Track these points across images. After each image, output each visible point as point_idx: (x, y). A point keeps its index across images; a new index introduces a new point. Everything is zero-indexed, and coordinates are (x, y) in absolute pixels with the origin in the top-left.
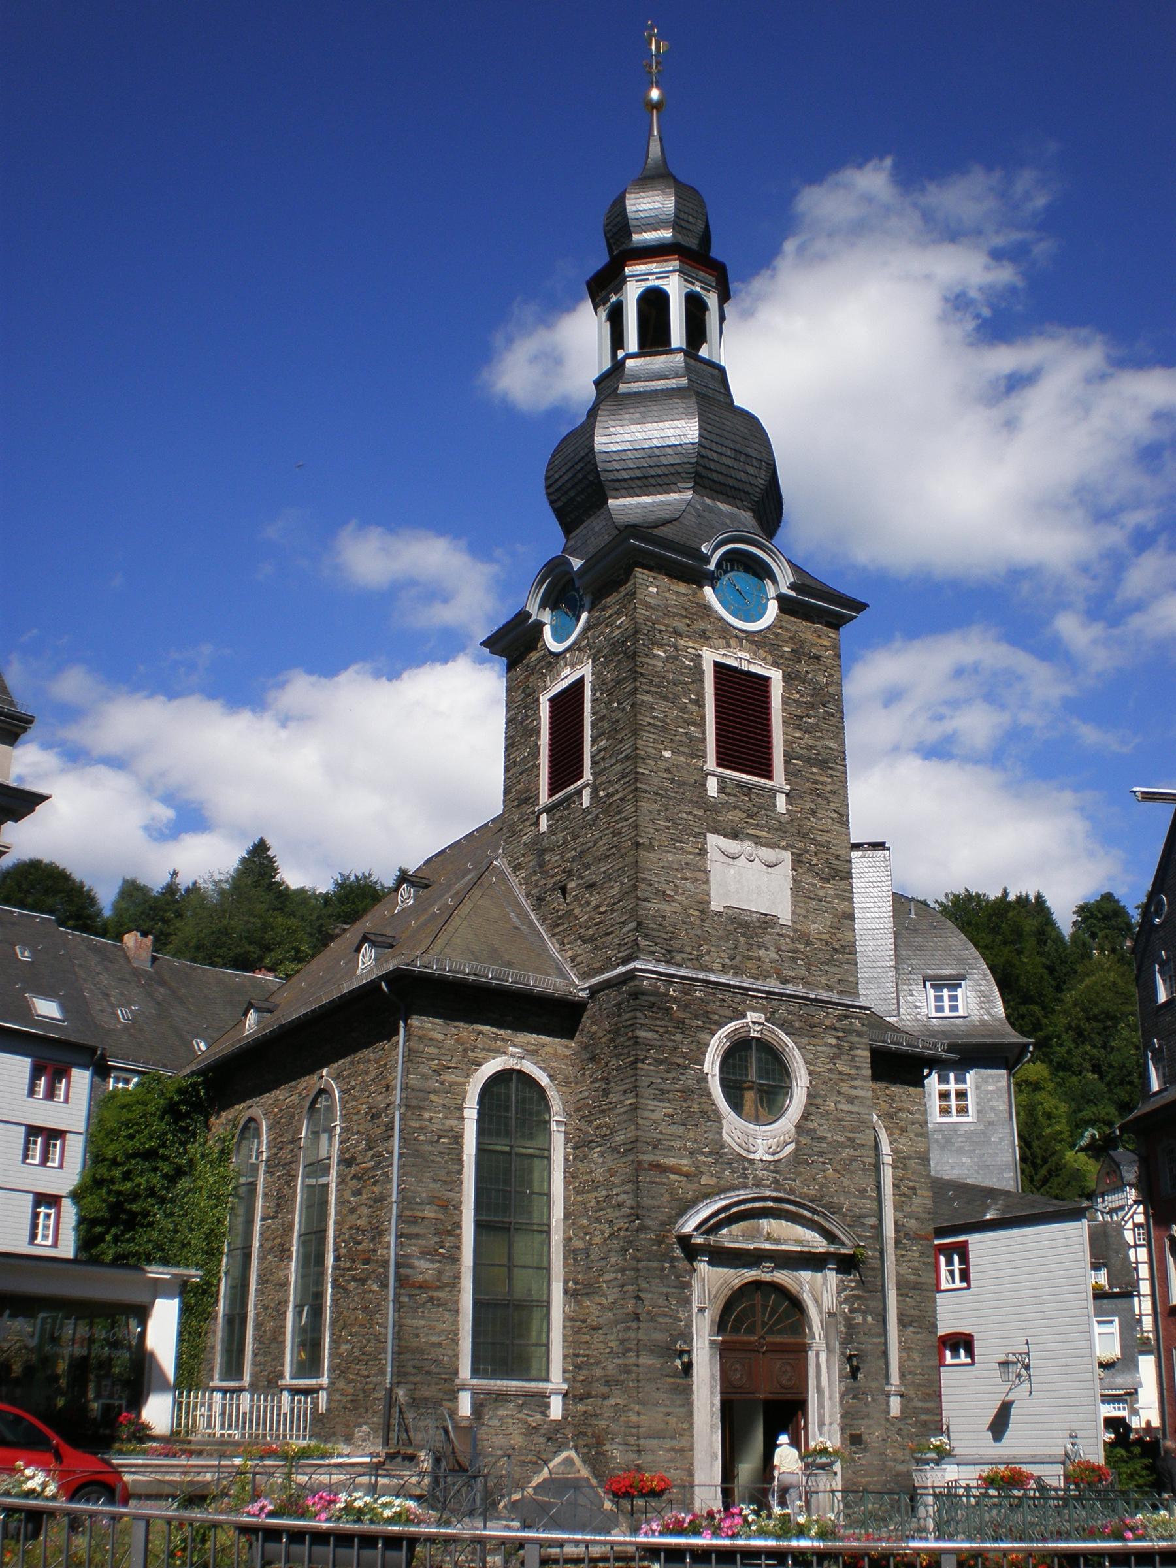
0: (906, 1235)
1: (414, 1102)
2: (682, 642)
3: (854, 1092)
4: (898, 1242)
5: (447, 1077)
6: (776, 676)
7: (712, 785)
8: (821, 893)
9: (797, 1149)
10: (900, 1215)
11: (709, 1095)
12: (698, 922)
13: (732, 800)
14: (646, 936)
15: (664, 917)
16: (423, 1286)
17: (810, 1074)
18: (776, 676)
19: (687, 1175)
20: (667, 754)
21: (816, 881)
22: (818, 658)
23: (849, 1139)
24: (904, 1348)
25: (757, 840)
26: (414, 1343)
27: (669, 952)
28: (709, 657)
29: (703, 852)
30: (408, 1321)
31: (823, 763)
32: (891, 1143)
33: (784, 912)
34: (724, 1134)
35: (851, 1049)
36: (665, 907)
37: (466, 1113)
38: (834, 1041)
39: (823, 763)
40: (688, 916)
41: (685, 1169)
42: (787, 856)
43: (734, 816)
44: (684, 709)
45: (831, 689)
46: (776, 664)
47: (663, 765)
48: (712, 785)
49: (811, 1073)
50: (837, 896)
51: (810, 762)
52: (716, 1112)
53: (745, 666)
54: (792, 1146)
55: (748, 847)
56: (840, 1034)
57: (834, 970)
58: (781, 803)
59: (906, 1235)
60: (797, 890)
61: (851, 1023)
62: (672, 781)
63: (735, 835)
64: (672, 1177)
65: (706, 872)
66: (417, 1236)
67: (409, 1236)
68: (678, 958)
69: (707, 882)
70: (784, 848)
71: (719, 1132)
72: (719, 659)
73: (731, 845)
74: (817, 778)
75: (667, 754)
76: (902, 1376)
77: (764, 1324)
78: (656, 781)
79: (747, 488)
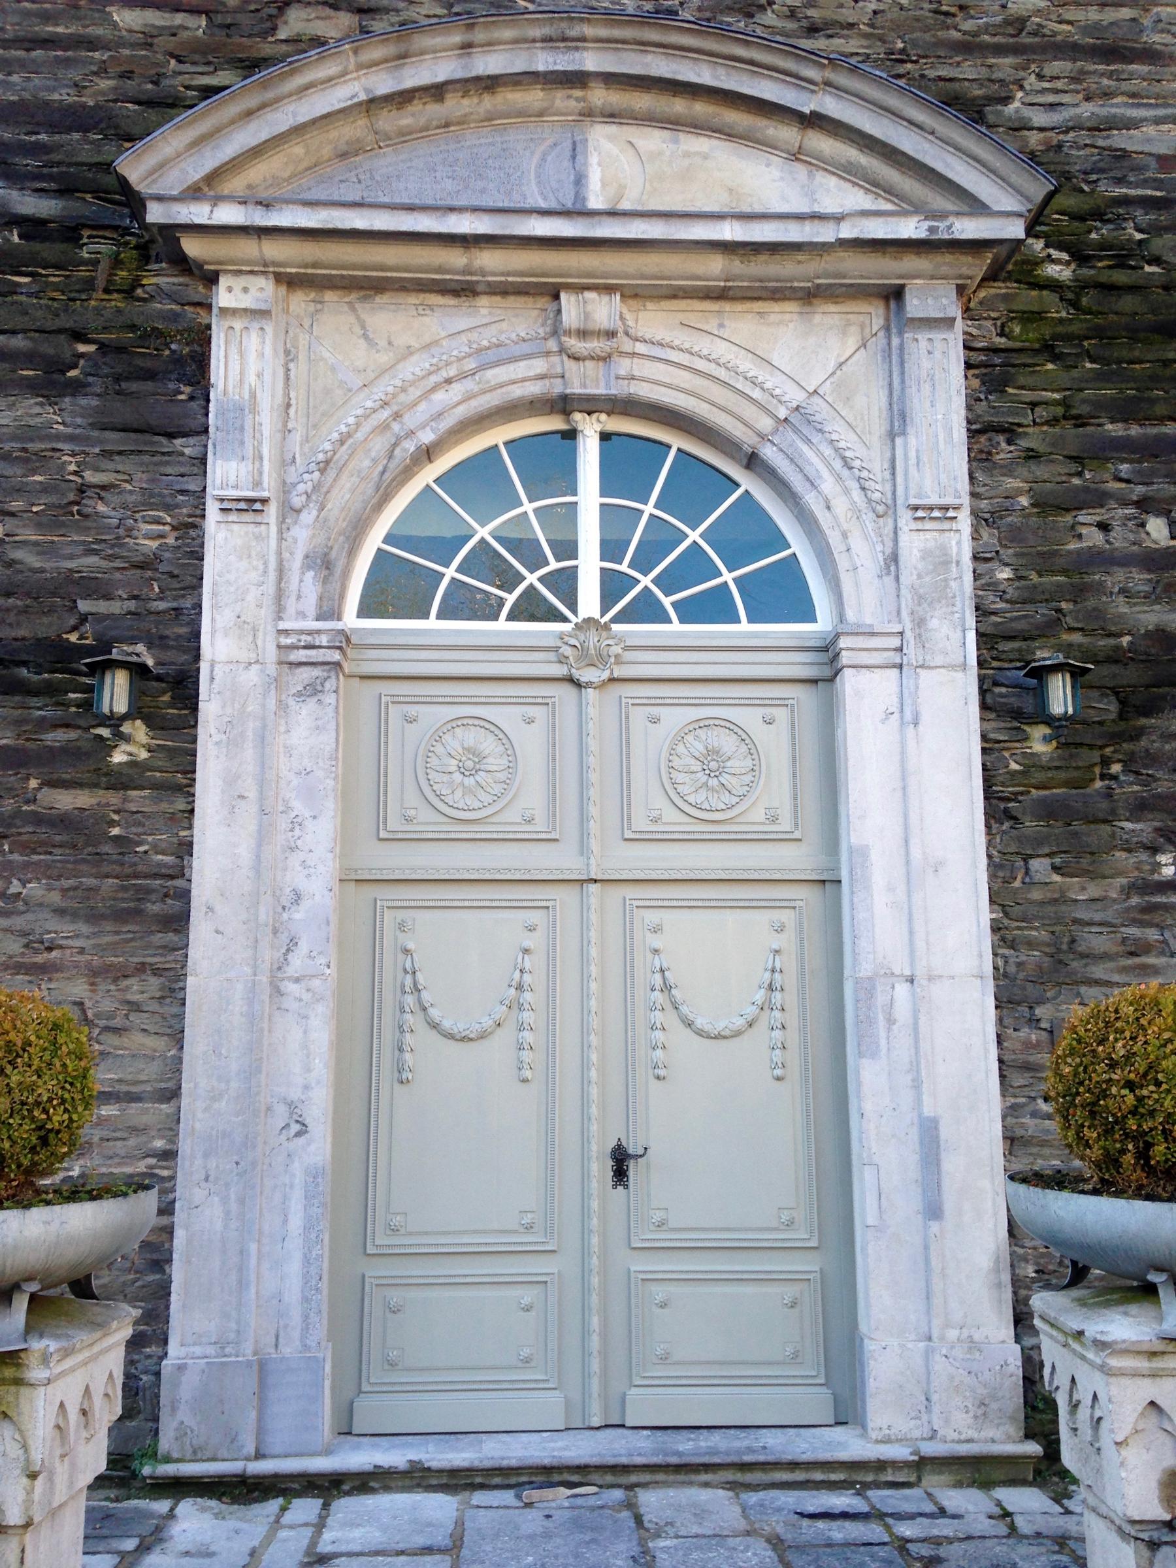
77: (612, 587)
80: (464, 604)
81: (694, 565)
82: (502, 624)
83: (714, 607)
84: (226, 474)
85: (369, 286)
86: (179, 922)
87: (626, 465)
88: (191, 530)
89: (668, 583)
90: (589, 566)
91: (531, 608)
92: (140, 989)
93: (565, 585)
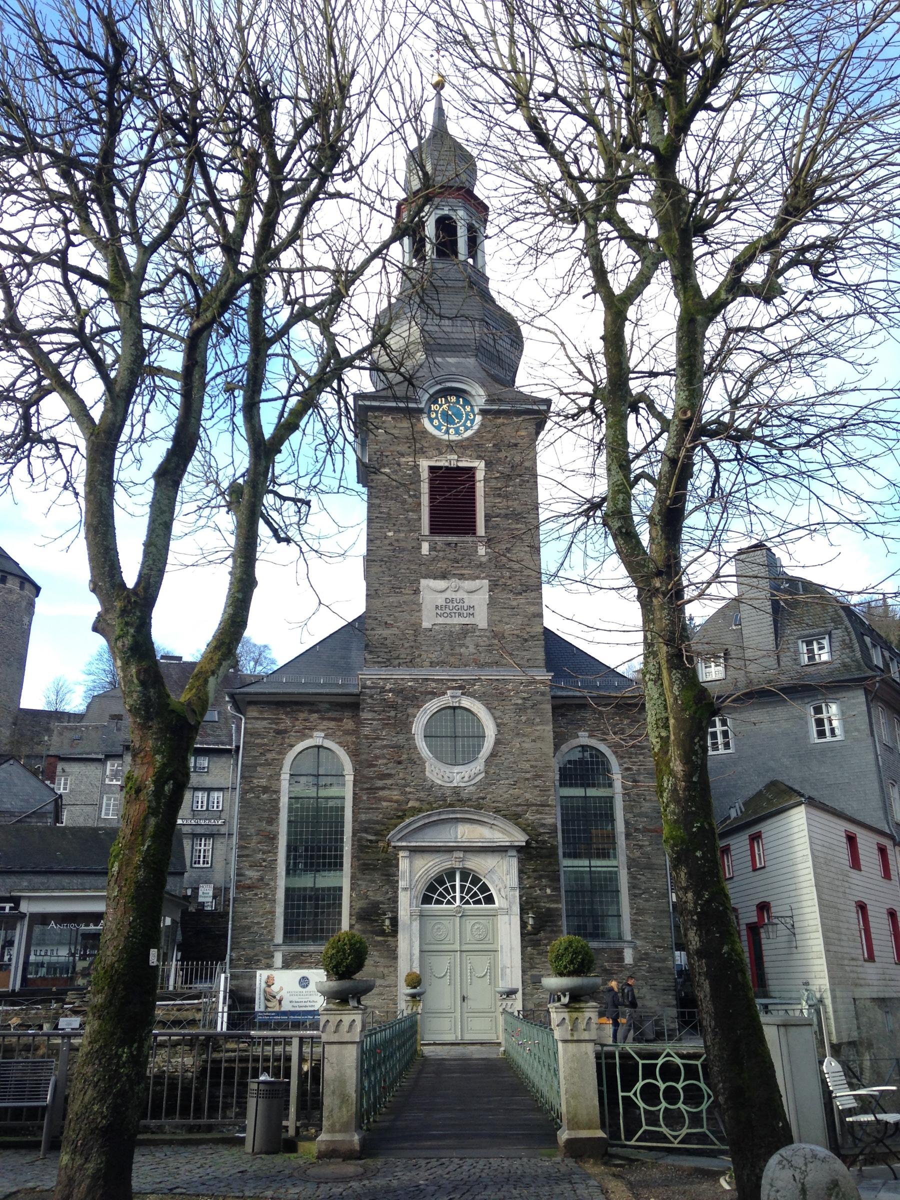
0: (636, 830)
1: (247, 774)
2: (403, 460)
3: (537, 734)
4: (628, 836)
5: (269, 756)
6: (480, 466)
7: (425, 548)
8: (514, 603)
9: (486, 777)
10: (629, 815)
11: (416, 748)
12: (412, 638)
13: (441, 554)
14: (371, 652)
15: (386, 639)
16: (249, 888)
17: (498, 726)
18: (480, 466)
19: (397, 801)
20: (390, 534)
21: (511, 596)
22: (516, 445)
23: (532, 766)
24: (637, 912)
25: (462, 577)
26: (244, 922)
27: (389, 660)
28: (424, 464)
29: (417, 592)
30: (240, 909)
31: (517, 516)
32: (621, 765)
33: (481, 619)
34: (427, 773)
35: (535, 705)
36: (386, 632)
37: (283, 776)
38: (520, 701)
39: (517, 516)
40: (404, 634)
41: (395, 798)
42: (486, 582)
43: (442, 565)
44: (404, 502)
45: (526, 464)
46: (479, 457)
47: (387, 542)
48: (425, 548)
49: (498, 725)
50: (529, 603)
51: (506, 516)
52: (420, 758)
53: (454, 464)
54: (483, 775)
55: (454, 582)
56: (525, 695)
57: (525, 653)
58: (482, 551)
59: (636, 830)
60: (492, 603)
61: (536, 688)
62: (394, 551)
63: (444, 576)
64: (385, 804)
65: (420, 605)
66: (247, 856)
67: (243, 856)
68: (396, 662)
69: (420, 611)
70: (483, 578)
71: (423, 771)
72: (433, 464)
73: (441, 584)
74: (513, 526)
75: (390, 534)
76: (635, 934)
77: (462, 898)
78: (382, 552)
79: (467, 342)
80: (439, 902)
81: (475, 895)
82: (444, 906)
83: (478, 902)
84: (402, 884)
85: (423, 851)
86: (396, 958)
87: (464, 879)
88: (396, 892)
89: (471, 897)
90: (458, 894)
91: (449, 903)
92: (391, 969)
93: (454, 898)
